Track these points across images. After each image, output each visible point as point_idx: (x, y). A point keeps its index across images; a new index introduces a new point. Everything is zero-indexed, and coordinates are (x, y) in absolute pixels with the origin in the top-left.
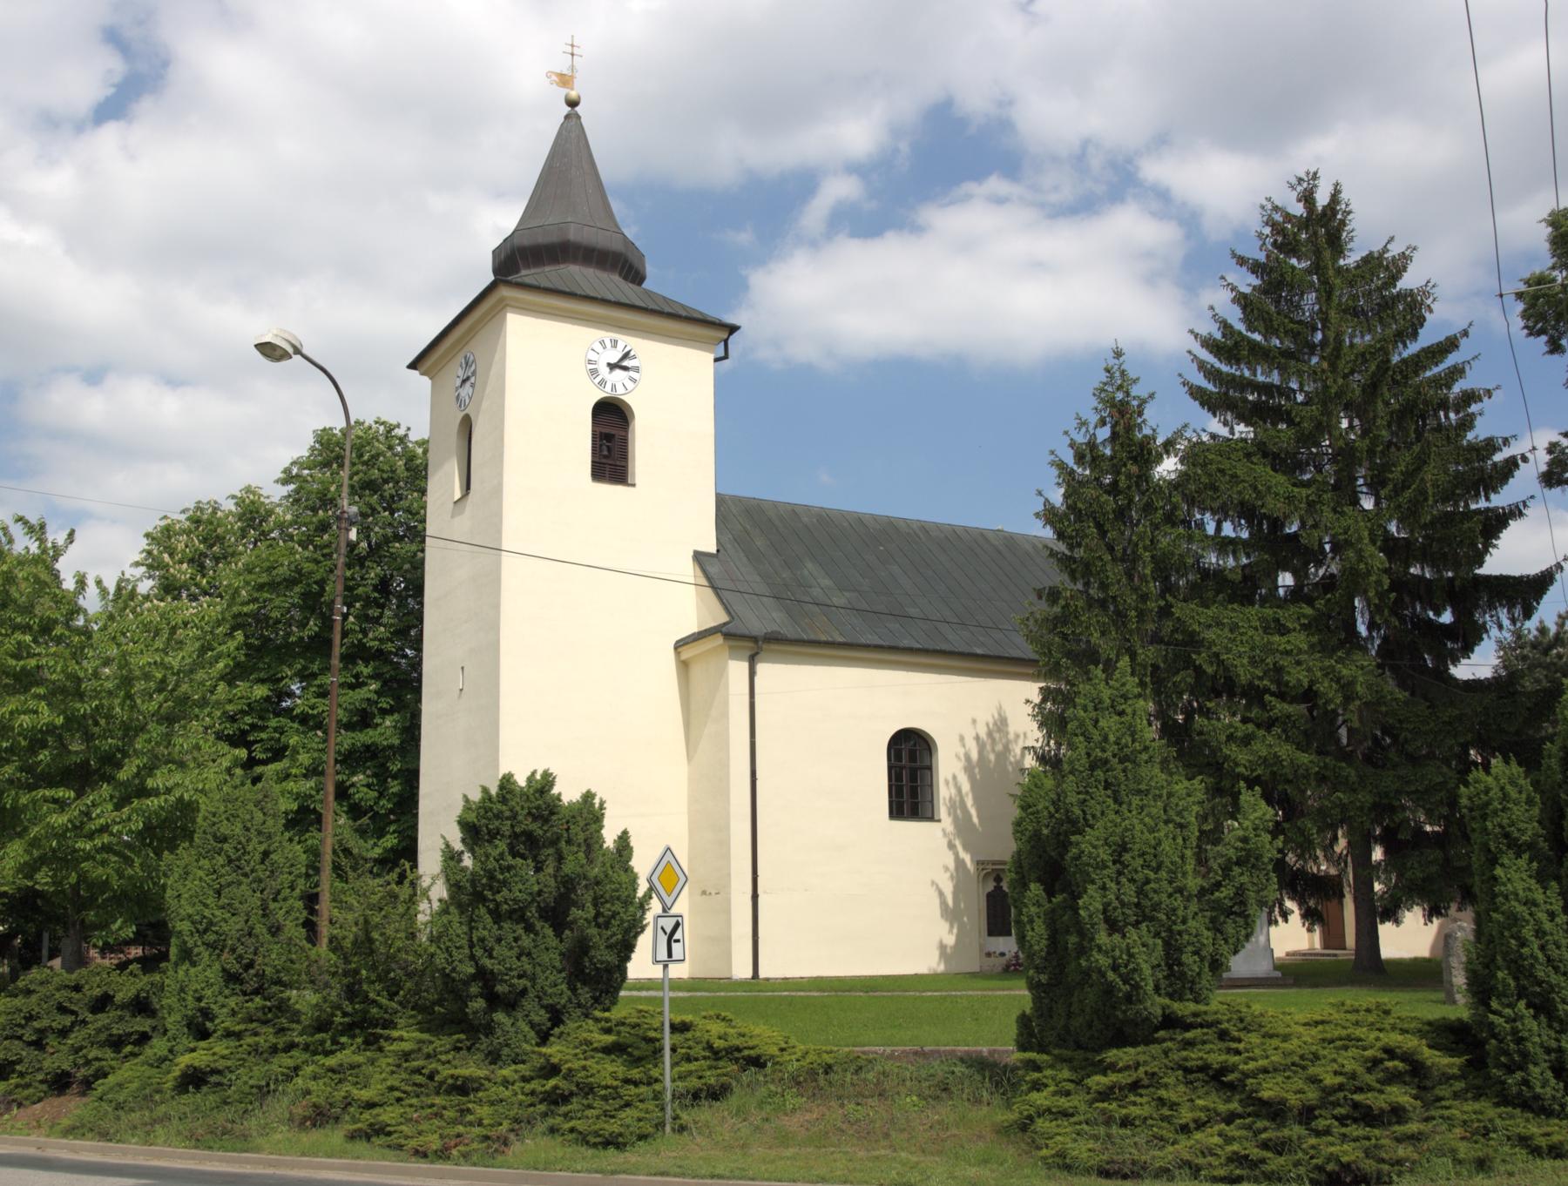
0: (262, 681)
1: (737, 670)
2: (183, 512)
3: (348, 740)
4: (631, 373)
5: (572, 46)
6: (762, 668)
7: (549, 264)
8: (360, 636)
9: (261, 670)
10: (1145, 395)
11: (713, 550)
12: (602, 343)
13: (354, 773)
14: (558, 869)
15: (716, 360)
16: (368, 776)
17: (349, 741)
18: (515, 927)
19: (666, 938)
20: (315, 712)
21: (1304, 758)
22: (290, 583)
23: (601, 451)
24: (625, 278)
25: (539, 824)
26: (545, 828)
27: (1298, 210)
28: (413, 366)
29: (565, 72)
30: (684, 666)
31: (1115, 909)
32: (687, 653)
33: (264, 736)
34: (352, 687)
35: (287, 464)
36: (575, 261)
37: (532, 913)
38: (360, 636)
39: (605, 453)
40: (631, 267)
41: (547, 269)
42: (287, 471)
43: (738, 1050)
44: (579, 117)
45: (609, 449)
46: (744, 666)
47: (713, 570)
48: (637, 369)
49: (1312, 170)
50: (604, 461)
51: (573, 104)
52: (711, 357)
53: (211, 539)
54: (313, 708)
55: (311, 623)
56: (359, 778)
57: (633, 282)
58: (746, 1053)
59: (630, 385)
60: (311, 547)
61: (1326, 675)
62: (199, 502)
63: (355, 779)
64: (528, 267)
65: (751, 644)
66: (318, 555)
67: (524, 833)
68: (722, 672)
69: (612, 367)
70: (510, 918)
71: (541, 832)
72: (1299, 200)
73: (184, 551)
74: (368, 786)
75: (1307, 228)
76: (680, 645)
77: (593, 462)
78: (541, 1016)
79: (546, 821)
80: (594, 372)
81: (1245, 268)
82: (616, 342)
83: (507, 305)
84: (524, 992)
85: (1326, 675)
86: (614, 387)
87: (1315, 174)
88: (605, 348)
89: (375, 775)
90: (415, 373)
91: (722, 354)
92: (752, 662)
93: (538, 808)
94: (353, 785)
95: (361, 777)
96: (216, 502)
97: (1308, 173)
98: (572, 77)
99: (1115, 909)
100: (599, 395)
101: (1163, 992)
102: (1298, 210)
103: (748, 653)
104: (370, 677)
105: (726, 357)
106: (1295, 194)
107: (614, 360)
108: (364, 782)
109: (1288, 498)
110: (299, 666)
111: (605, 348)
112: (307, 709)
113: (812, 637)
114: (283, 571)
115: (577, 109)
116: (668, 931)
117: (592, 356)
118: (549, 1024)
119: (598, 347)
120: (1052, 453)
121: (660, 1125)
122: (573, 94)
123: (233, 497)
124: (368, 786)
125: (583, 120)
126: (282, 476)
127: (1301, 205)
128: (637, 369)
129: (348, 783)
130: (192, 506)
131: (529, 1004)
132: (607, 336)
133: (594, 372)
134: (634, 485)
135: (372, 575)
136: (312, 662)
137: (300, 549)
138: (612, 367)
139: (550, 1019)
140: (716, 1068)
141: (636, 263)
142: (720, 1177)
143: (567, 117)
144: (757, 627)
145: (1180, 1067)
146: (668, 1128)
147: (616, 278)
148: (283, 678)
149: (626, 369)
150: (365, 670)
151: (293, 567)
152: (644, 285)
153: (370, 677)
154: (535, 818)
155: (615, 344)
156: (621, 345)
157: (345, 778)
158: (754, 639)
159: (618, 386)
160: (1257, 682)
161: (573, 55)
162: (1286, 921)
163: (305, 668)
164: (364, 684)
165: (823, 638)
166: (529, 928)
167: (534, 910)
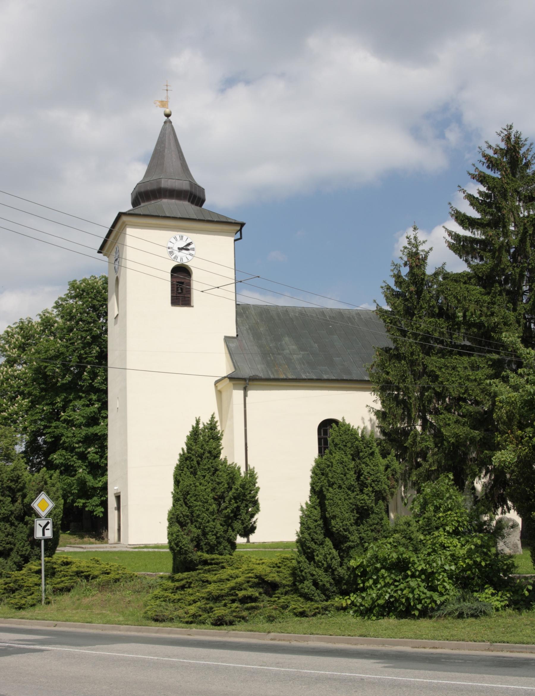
0: (47, 404)
1: (238, 394)
2: (14, 324)
3: (84, 431)
4: (191, 252)
5: (167, 86)
6: (250, 393)
7: (153, 200)
8: (90, 381)
9: (47, 399)
10: (427, 249)
11: (235, 335)
12: (175, 238)
13: (89, 447)
14: (22, 501)
15: (235, 240)
16: (96, 448)
17: (85, 432)
18: (6, 524)
19: (42, 528)
20: (71, 418)
21: (476, 433)
22: (56, 357)
23: (178, 290)
24: (192, 203)
25: (13, 483)
26: (16, 485)
27: (503, 146)
28: (99, 252)
29: (164, 100)
30: (219, 393)
31: (181, 517)
32: (220, 386)
33: (49, 430)
34: (88, 406)
35: (56, 299)
36: (165, 197)
37: (12, 518)
38: (90, 381)
39: (180, 291)
40: (195, 196)
41: (153, 202)
42: (57, 303)
43: (82, 572)
44: (171, 122)
45: (182, 289)
46: (242, 392)
47: (232, 345)
48: (193, 249)
49: (510, 124)
50: (178, 295)
51: (168, 115)
52: (232, 239)
53: (27, 337)
54: (70, 416)
55: (67, 376)
56: (91, 449)
57: (197, 205)
58: (85, 573)
59: (190, 257)
60: (64, 340)
61: (483, 392)
62: (21, 319)
63: (89, 450)
64: (144, 202)
65: (243, 382)
66: (68, 344)
67: (8, 487)
68: (230, 396)
69: (180, 249)
70: (3, 521)
71: (14, 486)
72: (502, 140)
73: (15, 343)
74: (96, 453)
75: (506, 155)
76: (217, 382)
77: (172, 296)
78: (18, 559)
79: (17, 481)
80: (171, 253)
81: (475, 180)
82: (182, 237)
83: (126, 225)
84: (11, 549)
85: (483, 392)
86: (182, 259)
87: (511, 126)
88: (177, 240)
89: (99, 447)
90: (101, 255)
91: (239, 237)
92: (245, 389)
93: (12, 477)
94: (89, 453)
95: (92, 449)
96: (30, 318)
97: (507, 126)
98: (167, 102)
99: (181, 517)
100: (174, 264)
101: (204, 550)
102: (503, 146)
103: (243, 386)
104: (95, 401)
105: (241, 238)
106: (500, 137)
107: (182, 246)
108: (94, 451)
109: (476, 301)
110: (63, 397)
111: (177, 240)
112: (66, 417)
113: (276, 377)
114: (52, 352)
115: (170, 118)
116: (43, 525)
117: (170, 245)
118: (23, 562)
119: (173, 240)
120: (384, 282)
121: (40, 601)
122: (168, 111)
123: (40, 315)
124: (96, 453)
125: (173, 124)
126: (55, 305)
127: (503, 143)
128: (193, 249)
129: (86, 452)
130: (18, 321)
131: (13, 554)
132: (177, 234)
133: (171, 253)
134: (193, 306)
135: (94, 352)
136: (70, 395)
137: (60, 342)
138: (180, 249)
139: (23, 560)
140: (72, 579)
141: (198, 194)
142: (38, 619)
143: (165, 122)
144: (247, 372)
145: (202, 580)
146: (43, 602)
147: (186, 203)
148: (56, 403)
149: (188, 250)
150: (94, 397)
151: (56, 351)
152: (204, 206)
153: (95, 401)
154: (12, 481)
155: (182, 238)
156: (185, 238)
157: (84, 450)
158: (244, 379)
159: (184, 258)
160: (461, 396)
161: (167, 90)
162: (509, 512)
163: (66, 398)
164: (93, 404)
165: (283, 376)
166: (12, 524)
167: (13, 517)
